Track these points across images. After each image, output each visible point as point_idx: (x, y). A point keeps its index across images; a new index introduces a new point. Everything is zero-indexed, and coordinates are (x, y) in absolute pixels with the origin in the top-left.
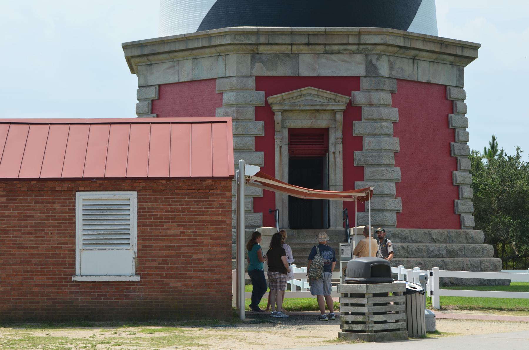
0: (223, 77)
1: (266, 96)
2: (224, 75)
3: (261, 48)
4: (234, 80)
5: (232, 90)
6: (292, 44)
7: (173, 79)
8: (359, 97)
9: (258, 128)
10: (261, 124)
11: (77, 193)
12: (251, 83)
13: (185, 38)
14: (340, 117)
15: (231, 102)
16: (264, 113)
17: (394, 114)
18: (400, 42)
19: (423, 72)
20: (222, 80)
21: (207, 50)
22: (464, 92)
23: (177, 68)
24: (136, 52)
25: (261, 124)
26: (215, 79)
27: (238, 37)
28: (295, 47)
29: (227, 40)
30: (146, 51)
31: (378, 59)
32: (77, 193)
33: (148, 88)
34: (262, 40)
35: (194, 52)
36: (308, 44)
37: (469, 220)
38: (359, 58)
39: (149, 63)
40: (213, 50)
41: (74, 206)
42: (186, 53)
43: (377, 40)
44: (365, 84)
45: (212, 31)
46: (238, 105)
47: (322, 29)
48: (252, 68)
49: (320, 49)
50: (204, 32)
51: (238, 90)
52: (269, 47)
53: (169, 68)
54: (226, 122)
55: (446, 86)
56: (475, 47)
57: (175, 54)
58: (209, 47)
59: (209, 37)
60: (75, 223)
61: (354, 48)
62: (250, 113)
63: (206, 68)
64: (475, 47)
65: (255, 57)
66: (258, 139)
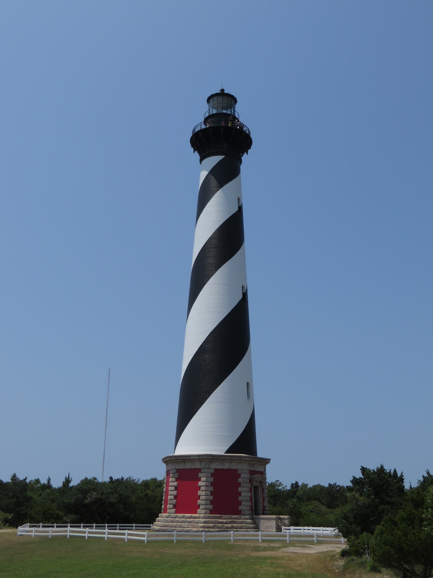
1: (251, 476)
7: (220, 467)
9: (249, 485)
12: (248, 472)
16: (250, 482)
26: (237, 470)
30: (215, 458)
40: (240, 461)
63: (234, 466)
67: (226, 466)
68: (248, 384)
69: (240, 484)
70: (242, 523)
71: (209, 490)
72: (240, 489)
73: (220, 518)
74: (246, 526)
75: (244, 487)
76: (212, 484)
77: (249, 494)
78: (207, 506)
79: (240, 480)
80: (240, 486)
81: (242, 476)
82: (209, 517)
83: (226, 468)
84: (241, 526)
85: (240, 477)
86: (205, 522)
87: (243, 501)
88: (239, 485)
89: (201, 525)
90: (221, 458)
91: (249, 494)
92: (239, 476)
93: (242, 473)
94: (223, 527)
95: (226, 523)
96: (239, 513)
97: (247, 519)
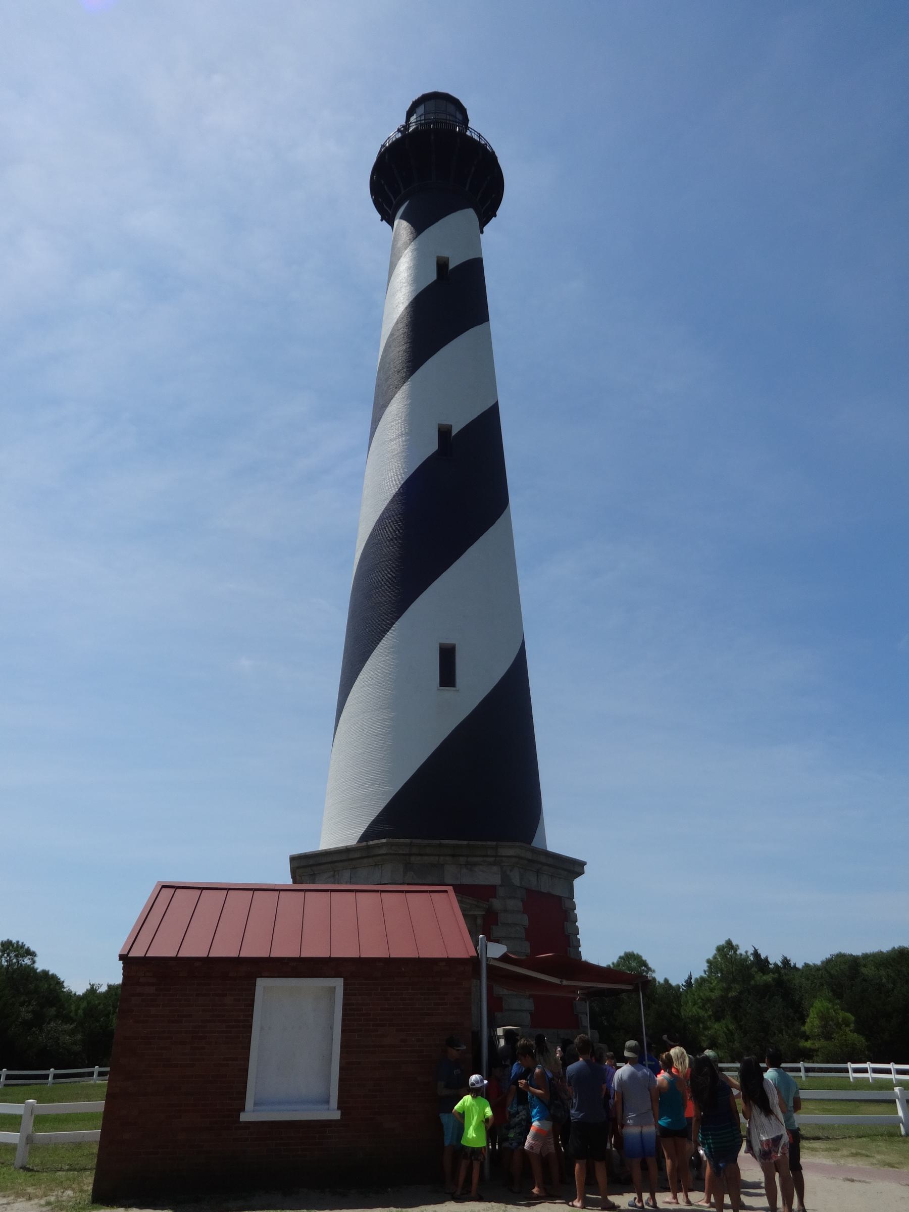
3: (413, 858)
6: (439, 855)
8: (497, 904)
11: (258, 980)
13: (347, 850)
14: (479, 921)
17: (525, 920)
18: (529, 856)
19: (546, 885)
21: (365, 861)
22: (574, 904)
28: (442, 858)
29: (383, 851)
30: (311, 862)
31: (511, 871)
32: (258, 980)
36: (453, 856)
37: (586, 1021)
38: (495, 869)
41: (253, 1000)
43: (511, 852)
44: (501, 892)
45: (371, 843)
47: (465, 842)
49: (462, 860)
50: (364, 844)
54: (446, 891)
55: (560, 898)
56: (583, 864)
58: (368, 857)
59: (368, 847)
60: (251, 1026)
61: (492, 859)
64: (583, 864)
68: (447, 656)
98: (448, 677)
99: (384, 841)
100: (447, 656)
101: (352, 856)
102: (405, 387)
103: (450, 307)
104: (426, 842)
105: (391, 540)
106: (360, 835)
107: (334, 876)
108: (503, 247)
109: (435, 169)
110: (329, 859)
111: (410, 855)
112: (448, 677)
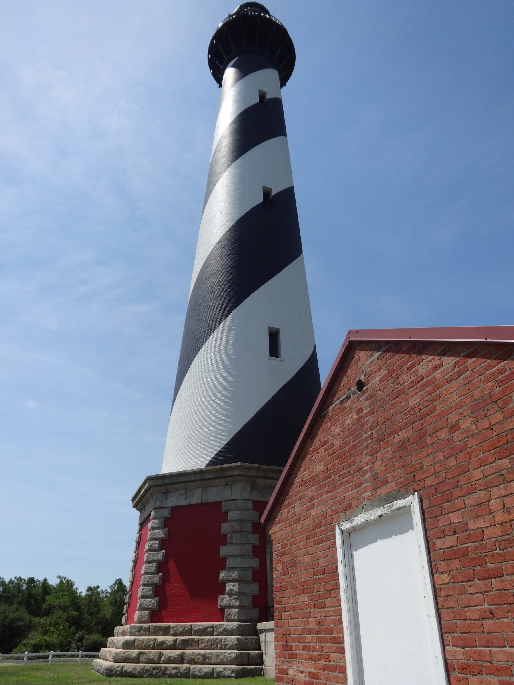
0: (228, 500)
2: (229, 499)
3: (259, 481)
4: (239, 502)
5: (236, 509)
7: (184, 502)
9: (254, 539)
10: (257, 536)
12: (250, 505)
13: (201, 472)
15: (236, 518)
20: (228, 502)
21: (217, 481)
23: (189, 494)
24: (159, 482)
25: (257, 536)
26: (220, 503)
27: (244, 470)
29: (235, 473)
30: (167, 481)
33: (162, 509)
34: (261, 474)
35: (207, 482)
39: (166, 491)
40: (223, 481)
42: (199, 483)
45: (225, 466)
46: (241, 521)
48: (251, 494)
51: (241, 509)
52: (262, 480)
53: (182, 494)
57: (190, 483)
59: (222, 469)
62: (249, 527)
63: (213, 495)
65: (254, 487)
66: (254, 547)
67: (196, 497)
69: (225, 536)
70: (212, 646)
71: (155, 558)
72: (224, 551)
73: (166, 631)
74: (217, 656)
75: (233, 544)
76: (164, 544)
77: (254, 563)
78: (146, 601)
79: (225, 527)
80: (225, 544)
81: (231, 515)
82: (148, 632)
83: (194, 502)
84: (205, 656)
85: (226, 521)
86: (127, 645)
87: (230, 581)
88: (223, 540)
89: (234, 653)
90: (180, 480)
91: (254, 563)
92: (224, 517)
93: (231, 510)
94: (160, 658)
95: (174, 646)
96: (220, 614)
97: (231, 633)
98: (274, 350)
99: (238, 464)
100: (274, 337)
101: (206, 476)
102: (229, 169)
103: (259, 124)
104: (270, 467)
105: (229, 255)
106: (207, 462)
107: (186, 493)
108: (294, 97)
109: (251, 43)
110: (184, 479)
111: (257, 477)
112: (274, 350)
